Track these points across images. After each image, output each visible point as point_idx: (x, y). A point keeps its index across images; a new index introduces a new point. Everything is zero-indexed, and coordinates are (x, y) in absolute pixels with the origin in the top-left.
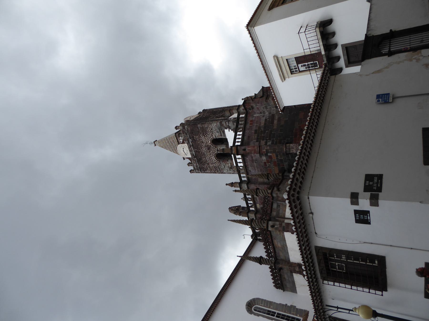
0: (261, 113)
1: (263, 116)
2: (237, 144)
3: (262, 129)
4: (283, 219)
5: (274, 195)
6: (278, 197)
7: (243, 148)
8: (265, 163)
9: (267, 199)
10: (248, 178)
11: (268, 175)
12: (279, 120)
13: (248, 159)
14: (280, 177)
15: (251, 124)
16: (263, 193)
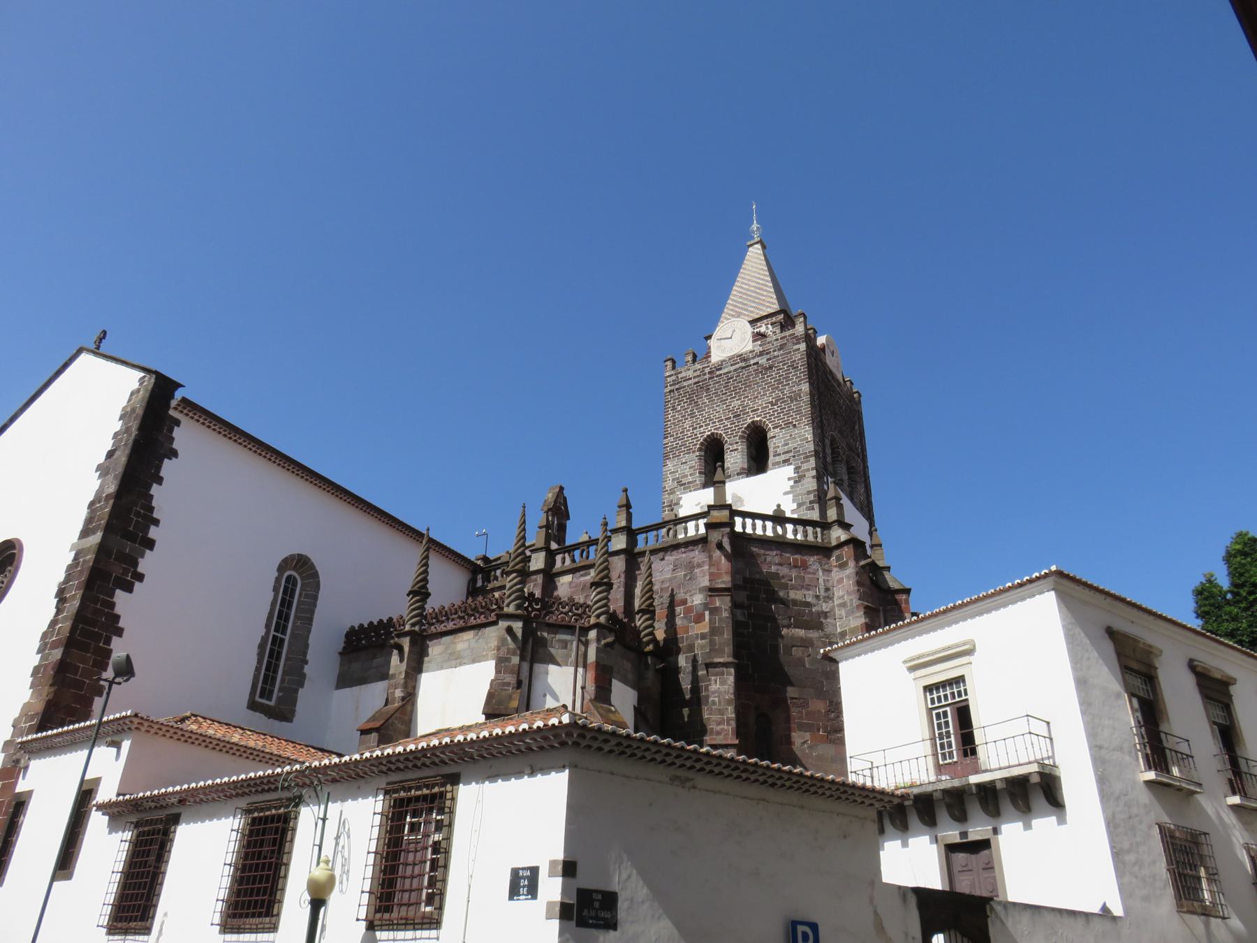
0: (827, 590)
2: (738, 520)
4: (529, 658)
9: (584, 612)
12: (806, 643)
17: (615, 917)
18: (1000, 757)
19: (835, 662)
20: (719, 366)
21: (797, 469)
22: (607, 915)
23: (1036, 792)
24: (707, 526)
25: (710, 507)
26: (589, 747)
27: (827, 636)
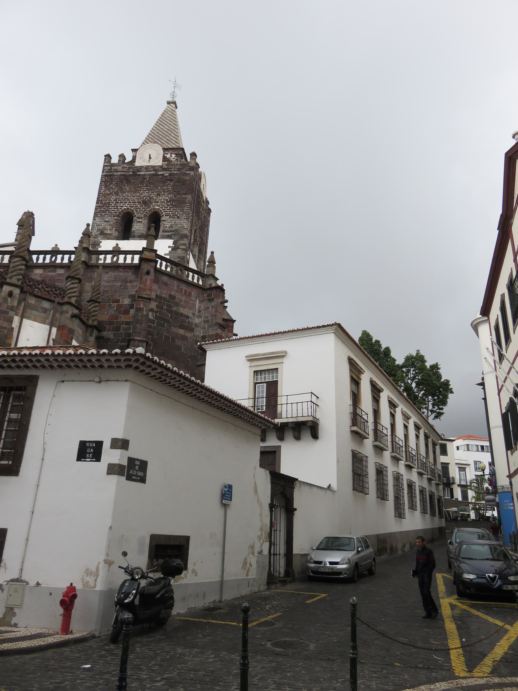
0: (199, 311)
1: (194, 314)
3: (174, 309)
4: (20, 314)
5: (65, 308)
6: (62, 313)
7: (152, 271)
8: (118, 301)
9: (60, 294)
10: (97, 266)
11: (97, 302)
13: (130, 275)
14: (90, 322)
15: (186, 291)
16: (72, 288)
17: (145, 476)
18: (289, 411)
19: (205, 352)
20: (140, 168)
21: (174, 243)
22: (141, 474)
23: (307, 429)
24: (141, 259)
25: (143, 248)
26: (142, 371)
27: (195, 336)
